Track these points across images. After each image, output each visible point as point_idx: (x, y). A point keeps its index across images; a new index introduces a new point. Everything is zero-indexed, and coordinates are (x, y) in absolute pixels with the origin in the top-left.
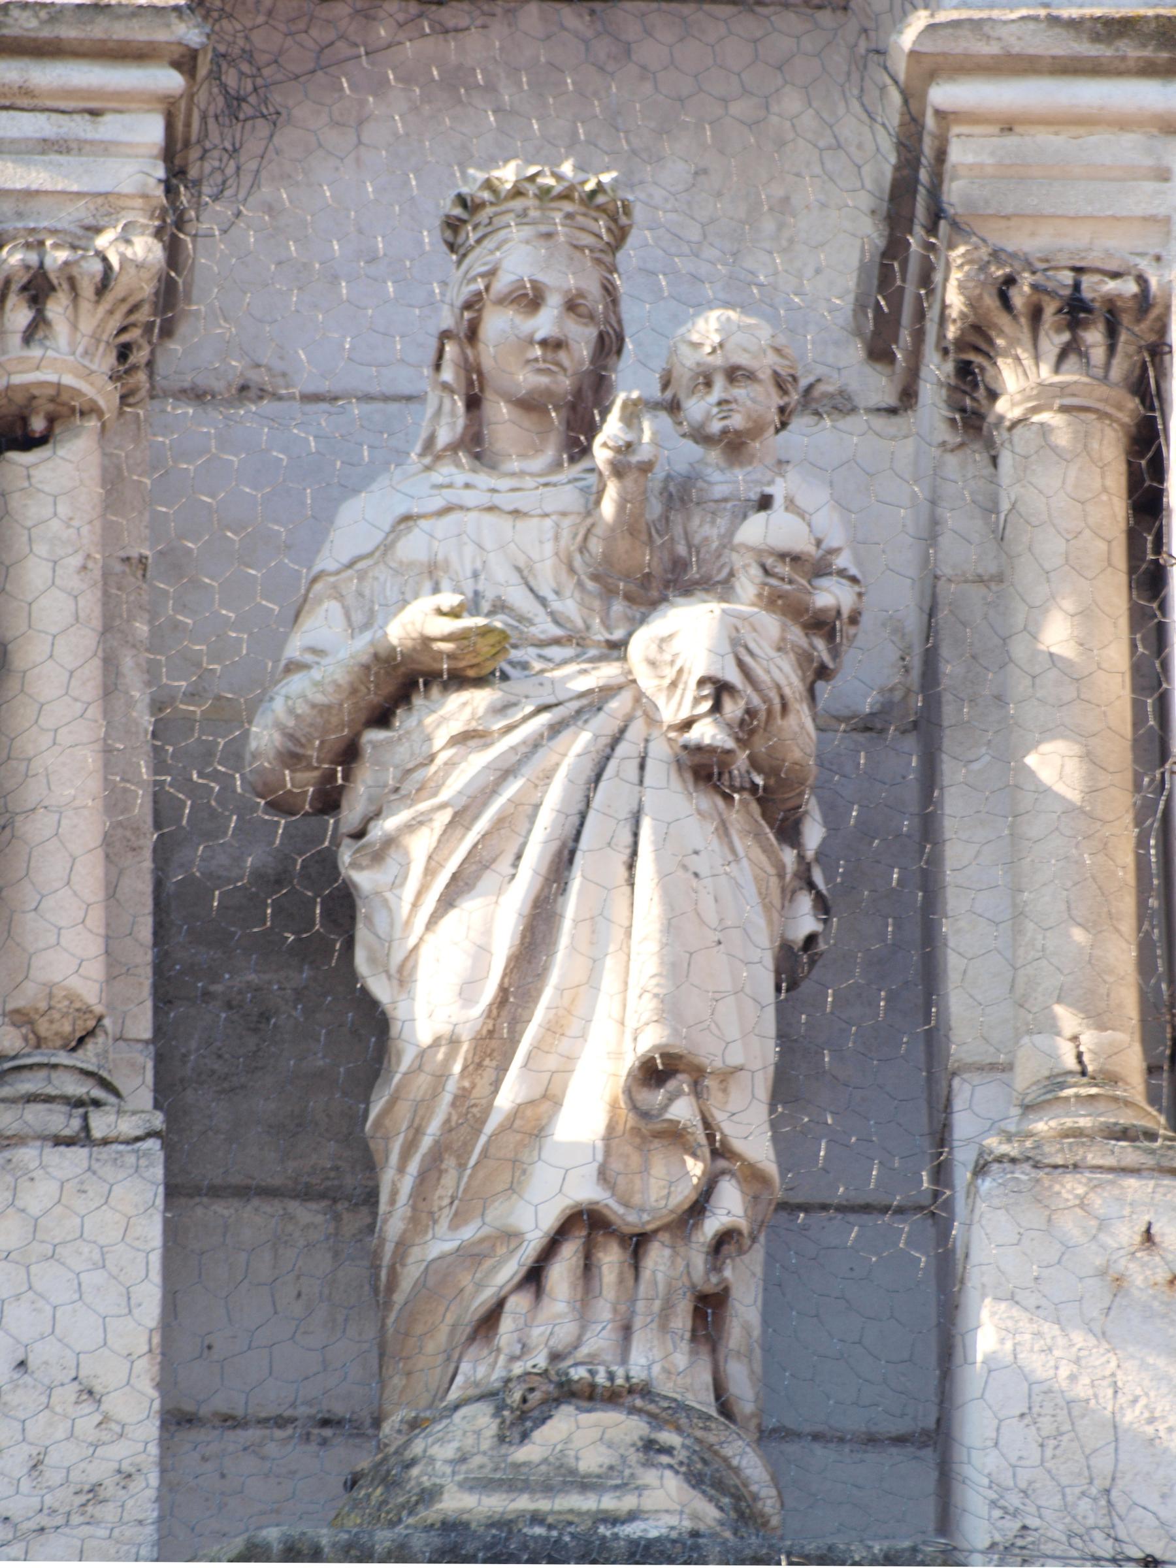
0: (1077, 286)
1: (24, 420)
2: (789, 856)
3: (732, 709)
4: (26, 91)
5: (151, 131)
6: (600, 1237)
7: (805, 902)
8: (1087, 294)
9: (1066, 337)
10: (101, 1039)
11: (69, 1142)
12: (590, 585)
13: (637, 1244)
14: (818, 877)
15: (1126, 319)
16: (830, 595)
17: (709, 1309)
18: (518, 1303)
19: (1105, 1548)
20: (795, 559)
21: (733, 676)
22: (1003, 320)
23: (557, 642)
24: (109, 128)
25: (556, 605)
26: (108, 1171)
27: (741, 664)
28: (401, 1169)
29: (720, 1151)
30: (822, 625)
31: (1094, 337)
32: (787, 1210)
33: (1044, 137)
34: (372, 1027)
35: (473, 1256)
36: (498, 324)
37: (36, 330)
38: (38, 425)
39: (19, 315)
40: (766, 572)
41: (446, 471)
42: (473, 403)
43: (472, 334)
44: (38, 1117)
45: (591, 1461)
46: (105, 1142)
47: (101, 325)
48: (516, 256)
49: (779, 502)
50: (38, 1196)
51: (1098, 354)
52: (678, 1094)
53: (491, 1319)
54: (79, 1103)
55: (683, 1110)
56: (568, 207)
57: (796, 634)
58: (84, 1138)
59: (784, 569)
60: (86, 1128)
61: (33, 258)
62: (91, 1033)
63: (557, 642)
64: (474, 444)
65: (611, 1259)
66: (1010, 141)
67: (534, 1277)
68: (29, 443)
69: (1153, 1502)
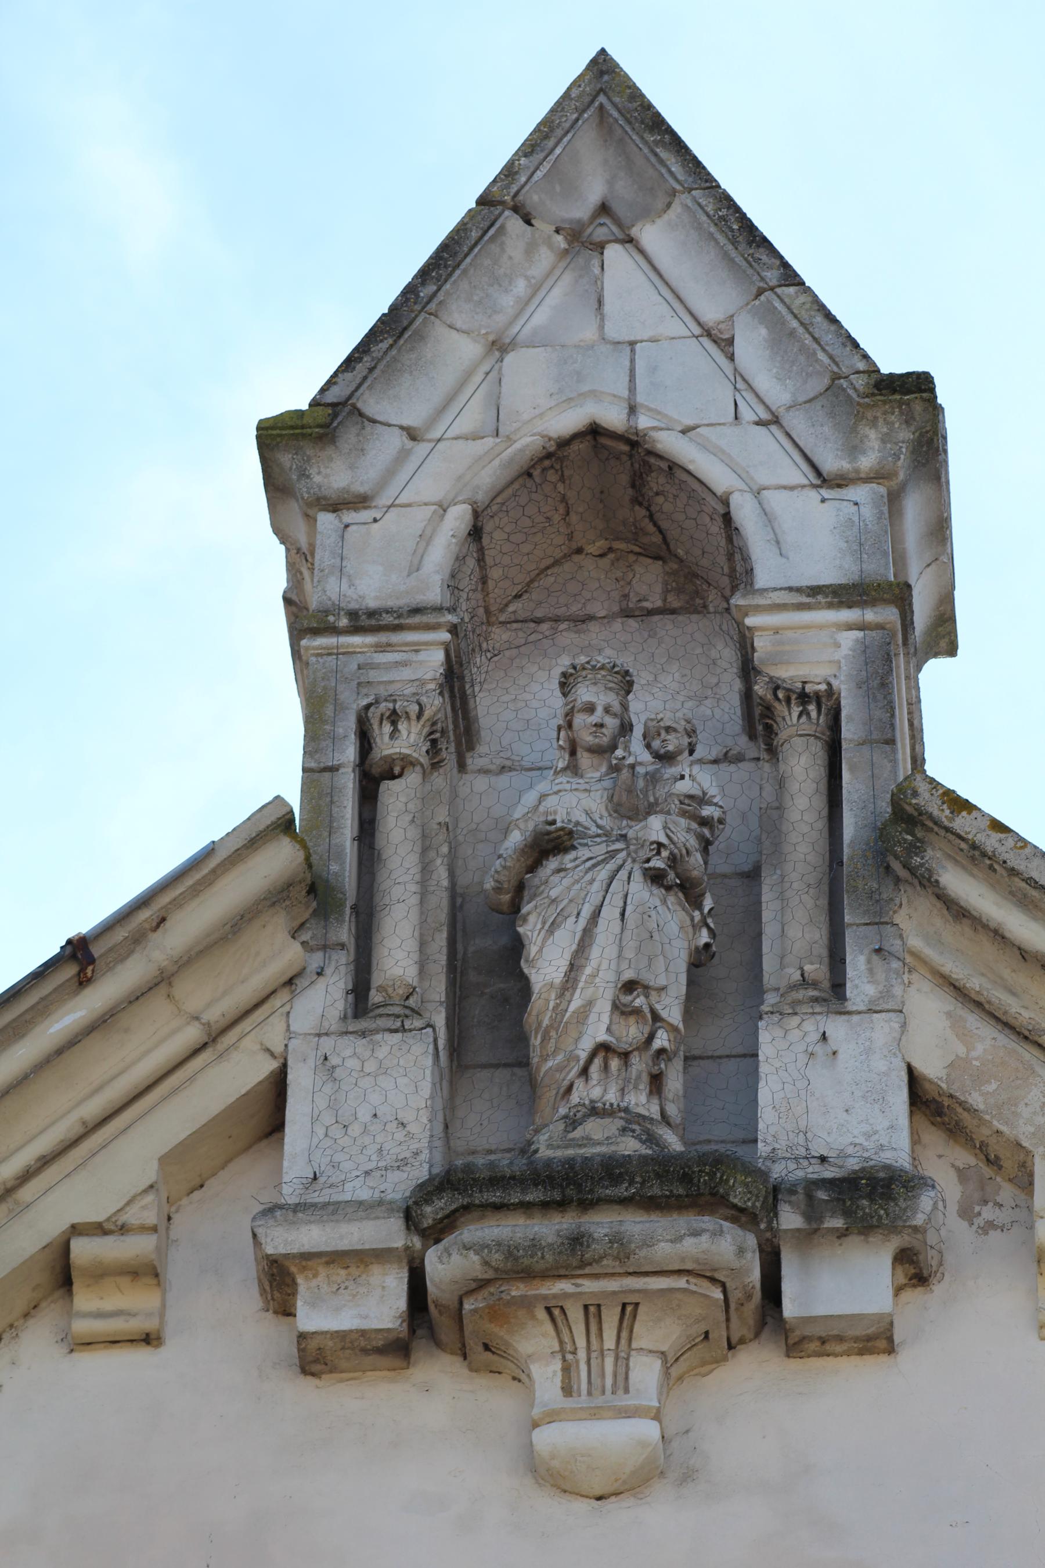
0: (804, 688)
1: (392, 769)
2: (697, 914)
3: (665, 853)
4: (389, 645)
5: (439, 656)
6: (610, 1055)
7: (705, 932)
8: (807, 690)
9: (801, 708)
10: (415, 996)
11: (396, 1031)
12: (615, 815)
13: (625, 1056)
14: (709, 921)
15: (824, 700)
16: (707, 811)
17: (656, 1082)
18: (579, 1084)
19: (802, 1152)
20: (691, 797)
21: (663, 840)
22: (776, 704)
23: (598, 836)
24: (422, 656)
25: (599, 822)
26: (411, 1041)
27: (668, 836)
28: (536, 1038)
29: (656, 1017)
30: (704, 822)
31: (812, 708)
33: (790, 634)
35: (560, 1068)
36: (579, 719)
37: (394, 734)
38: (397, 770)
39: (387, 728)
40: (681, 803)
41: (562, 779)
42: (573, 753)
43: (570, 725)
44: (382, 1023)
45: (597, 1136)
46: (410, 1030)
47: (421, 731)
48: (584, 693)
49: (687, 777)
50: (382, 1052)
51: (814, 714)
52: (638, 996)
53: (569, 1089)
54: (398, 1016)
55: (640, 1001)
56: (603, 673)
57: (694, 825)
58: (403, 1029)
59: (687, 801)
60: (403, 1026)
61: (391, 705)
62: (411, 994)
63: (598, 836)
64: (573, 768)
65: (615, 1063)
66: (778, 637)
67: (585, 1072)
68: (393, 777)
69: (825, 1136)
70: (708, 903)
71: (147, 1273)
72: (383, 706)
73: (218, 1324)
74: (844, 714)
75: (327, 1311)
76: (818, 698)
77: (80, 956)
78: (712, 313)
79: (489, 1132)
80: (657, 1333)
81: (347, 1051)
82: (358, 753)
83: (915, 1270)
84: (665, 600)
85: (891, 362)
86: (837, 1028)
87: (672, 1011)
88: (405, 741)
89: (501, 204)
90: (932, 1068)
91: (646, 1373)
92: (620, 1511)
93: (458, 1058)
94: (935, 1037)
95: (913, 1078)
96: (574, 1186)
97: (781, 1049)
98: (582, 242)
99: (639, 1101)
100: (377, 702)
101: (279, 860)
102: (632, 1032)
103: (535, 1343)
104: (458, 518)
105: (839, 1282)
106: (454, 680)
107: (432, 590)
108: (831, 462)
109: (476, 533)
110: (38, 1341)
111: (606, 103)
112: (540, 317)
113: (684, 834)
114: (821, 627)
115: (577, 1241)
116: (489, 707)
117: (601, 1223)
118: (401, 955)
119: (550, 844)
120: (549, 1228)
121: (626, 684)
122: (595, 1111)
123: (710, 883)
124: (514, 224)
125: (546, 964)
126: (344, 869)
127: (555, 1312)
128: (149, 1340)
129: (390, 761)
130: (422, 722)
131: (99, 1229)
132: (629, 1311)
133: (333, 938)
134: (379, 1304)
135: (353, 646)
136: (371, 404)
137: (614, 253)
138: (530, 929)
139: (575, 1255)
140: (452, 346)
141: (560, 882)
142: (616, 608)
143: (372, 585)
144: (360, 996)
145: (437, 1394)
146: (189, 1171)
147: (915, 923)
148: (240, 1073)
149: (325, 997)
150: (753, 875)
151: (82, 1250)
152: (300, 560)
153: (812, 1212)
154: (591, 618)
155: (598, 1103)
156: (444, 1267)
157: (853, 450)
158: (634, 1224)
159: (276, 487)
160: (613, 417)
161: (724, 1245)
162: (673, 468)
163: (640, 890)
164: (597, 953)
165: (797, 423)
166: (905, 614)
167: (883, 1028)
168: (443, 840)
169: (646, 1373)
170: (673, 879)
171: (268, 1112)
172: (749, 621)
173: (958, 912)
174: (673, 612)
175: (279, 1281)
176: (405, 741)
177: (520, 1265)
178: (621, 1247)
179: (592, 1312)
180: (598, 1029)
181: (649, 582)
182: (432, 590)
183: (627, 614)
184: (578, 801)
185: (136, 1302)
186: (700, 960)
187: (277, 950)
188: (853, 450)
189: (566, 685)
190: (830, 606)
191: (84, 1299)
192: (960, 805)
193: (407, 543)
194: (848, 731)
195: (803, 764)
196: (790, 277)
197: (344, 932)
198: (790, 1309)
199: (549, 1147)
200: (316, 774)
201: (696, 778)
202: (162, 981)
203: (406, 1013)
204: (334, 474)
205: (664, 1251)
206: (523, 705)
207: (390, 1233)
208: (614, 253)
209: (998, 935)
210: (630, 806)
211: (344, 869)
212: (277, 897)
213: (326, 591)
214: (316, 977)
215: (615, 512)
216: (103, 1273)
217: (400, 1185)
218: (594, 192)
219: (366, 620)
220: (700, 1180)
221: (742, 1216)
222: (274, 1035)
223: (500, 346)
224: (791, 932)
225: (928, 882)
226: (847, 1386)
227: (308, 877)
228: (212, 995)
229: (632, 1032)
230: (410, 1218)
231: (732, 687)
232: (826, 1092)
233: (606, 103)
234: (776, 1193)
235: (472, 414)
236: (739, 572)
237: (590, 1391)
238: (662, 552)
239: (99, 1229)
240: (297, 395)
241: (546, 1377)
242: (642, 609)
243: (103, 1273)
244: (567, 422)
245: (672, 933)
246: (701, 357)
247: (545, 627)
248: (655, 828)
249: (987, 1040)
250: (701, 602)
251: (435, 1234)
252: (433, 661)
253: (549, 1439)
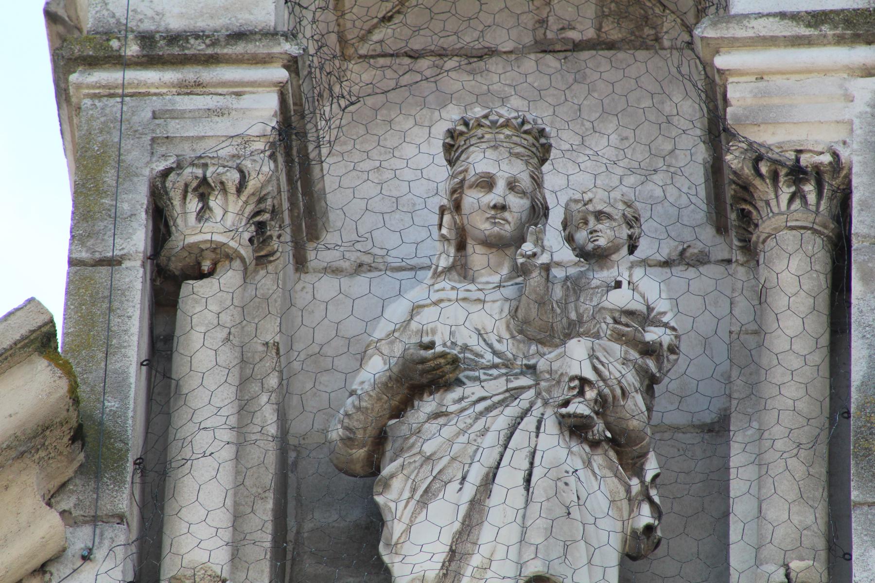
0: (798, 160)
1: (199, 264)
2: (635, 482)
3: (590, 394)
4: (199, 84)
5: (270, 102)
7: (646, 509)
9: (793, 189)
12: (519, 337)
14: (653, 492)
15: (827, 177)
16: (652, 335)
20: (630, 313)
21: (590, 374)
22: (757, 182)
23: (495, 366)
24: (246, 102)
25: (497, 346)
27: (595, 369)
30: (649, 350)
31: (809, 188)
36: (472, 199)
37: (203, 213)
38: (206, 266)
39: (194, 204)
40: (616, 321)
42: (461, 247)
43: (457, 206)
48: (479, 160)
49: (625, 284)
51: (812, 198)
56: (507, 132)
57: (634, 355)
59: (624, 320)
61: (199, 172)
63: (495, 366)
64: (461, 269)
66: (761, 84)
68: (201, 276)
70: (652, 467)
72: (189, 173)
74: (856, 198)
76: (818, 174)
84: (599, 29)
88: (221, 224)
100: (179, 166)
106: (291, 137)
113: (619, 367)
114: (826, 72)
116: (342, 179)
119: (425, 376)
121: (540, 149)
126: (126, 405)
129: (197, 251)
130: (243, 198)
133: (106, 507)
135: (145, 84)
138: (394, 498)
141: (438, 431)
142: (528, 39)
150: (718, 429)
154: (492, 52)
163: (553, 446)
168: (272, 366)
172: (720, 62)
174: (611, 46)
176: (221, 224)
183: (544, 48)
184: (469, 317)
189: (453, 147)
190: (840, 40)
195: (793, 270)
197: (124, 498)
200: (89, 268)
201: (638, 286)
206: (392, 175)
210: (543, 324)
211: (126, 405)
214: (80, 562)
219: (163, 49)
231: (693, 156)
242: (565, 40)
247: (424, 64)
250: (652, 32)
252: (261, 110)
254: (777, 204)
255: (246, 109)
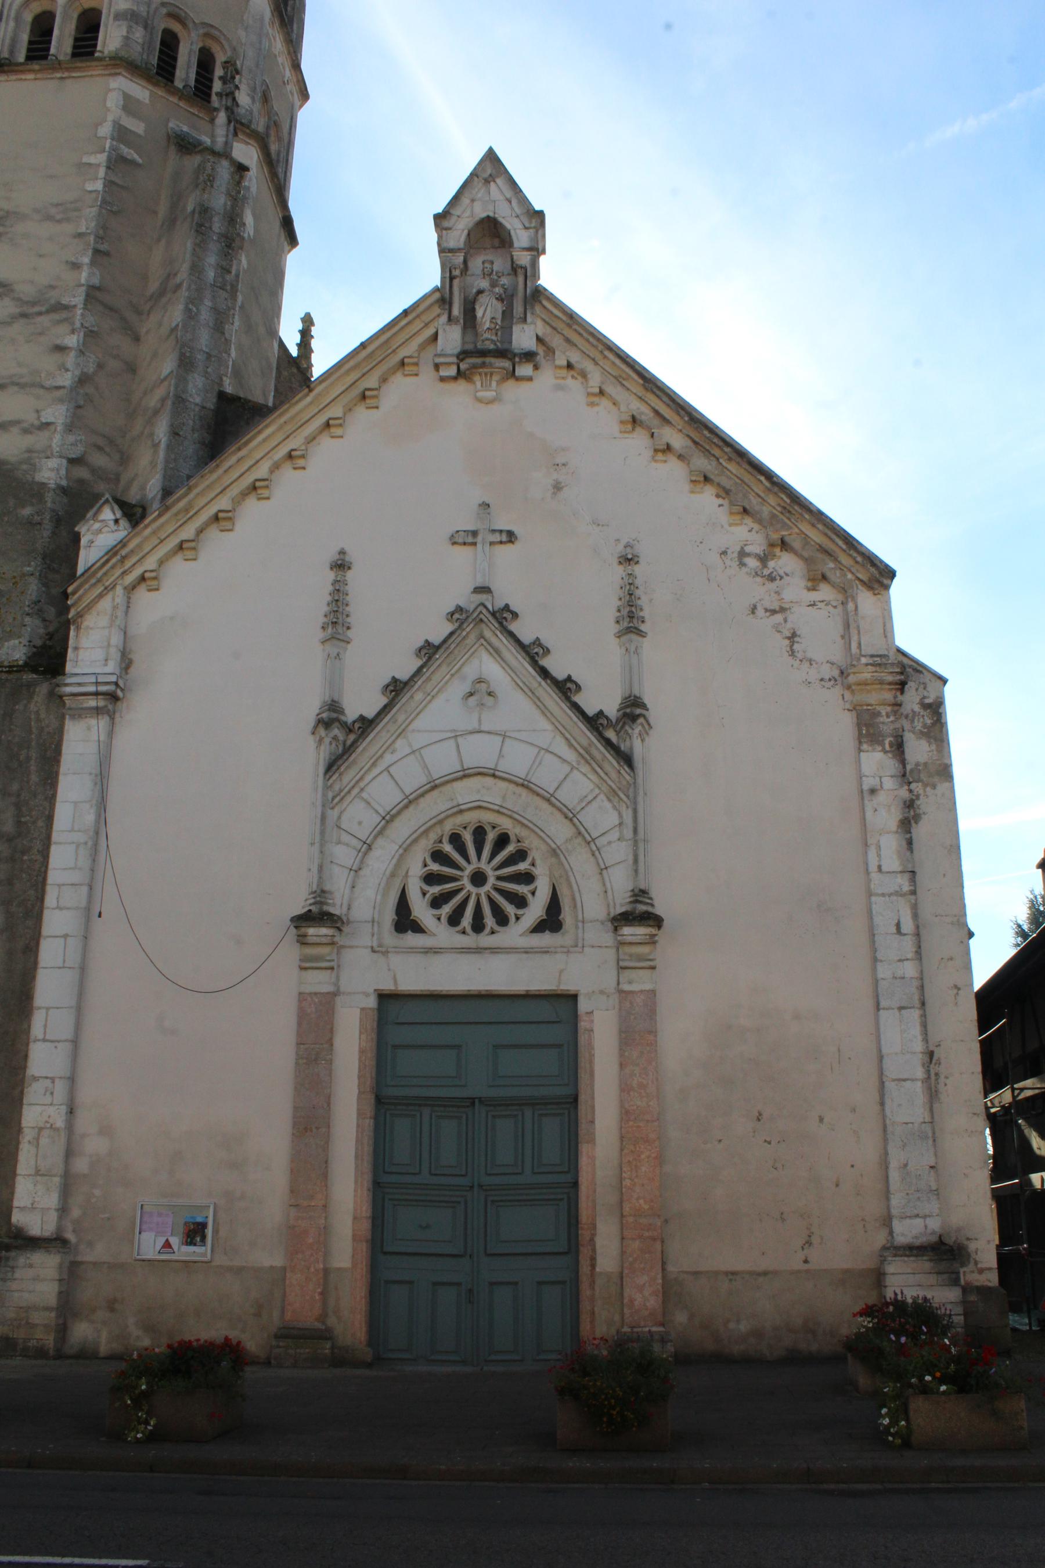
32: (502, 328)
34: (475, 317)
48: (486, 265)
71: (416, 364)
73: (427, 374)
75: (445, 372)
77: (406, 313)
78: (508, 196)
79: (470, 347)
80: (495, 378)
81: (447, 328)
82: (447, 269)
83: (536, 367)
85: (537, 208)
86: (525, 327)
87: (499, 322)
88: (457, 273)
89: (474, 175)
90: (540, 334)
91: (494, 384)
92: (490, 406)
93: (465, 328)
94: (540, 329)
95: (537, 336)
96: (483, 353)
97: (516, 329)
98: (487, 181)
99: (494, 338)
101: (437, 295)
102: (493, 326)
103: (477, 378)
104: (466, 232)
105: (525, 369)
106: (465, 262)
107: (462, 246)
108: (527, 225)
109: (469, 234)
110: (399, 374)
111: (491, 157)
112: (480, 195)
113: (502, 291)
115: (484, 363)
116: (470, 264)
117: (488, 360)
118: (456, 311)
119: (480, 292)
120: (479, 360)
121: (492, 263)
122: (487, 339)
123: (506, 299)
124: (476, 178)
125: (479, 313)
126: (447, 296)
127: (480, 374)
128: (416, 375)
131: (409, 357)
132: (491, 374)
134: (452, 371)
136: (452, 211)
137: (492, 183)
138: (477, 307)
139: (483, 365)
140: (465, 200)
141: (483, 299)
143: (452, 244)
144: (450, 319)
145: (462, 385)
146: (422, 347)
147: (538, 309)
148: (429, 332)
149: (444, 318)
150: (512, 296)
151: (406, 360)
152: (440, 237)
153: (521, 359)
155: (488, 339)
156: (463, 366)
157: (531, 223)
158: (493, 360)
159: (437, 225)
160: (491, 214)
161: (507, 364)
162: (501, 224)
163: (495, 301)
164: (488, 311)
165: (522, 217)
166: (537, 250)
167: (533, 326)
168: (463, 289)
169: (494, 384)
170: (500, 299)
171: (435, 337)
173: (544, 307)
175: (437, 367)
176: (457, 273)
177: (474, 367)
178: (491, 365)
179: (486, 374)
180: (487, 325)
181: (496, 242)
182: (462, 246)
184: (484, 284)
185: (414, 369)
186: (504, 312)
187: (437, 310)
188: (531, 223)
189: (483, 263)
191: (406, 368)
192: (546, 290)
193: (458, 238)
194: (529, 274)
195: (521, 279)
196: (521, 191)
197: (447, 307)
198: (517, 374)
199: (479, 346)
200: (443, 279)
201: (504, 281)
202: (418, 316)
203: (457, 322)
204: (446, 224)
205: (497, 365)
206: (477, 264)
207: (455, 360)
208: (492, 183)
209: (552, 313)
210: (494, 284)
211: (447, 296)
212: (437, 301)
213: (444, 245)
215: (491, 233)
216: (409, 364)
217: (456, 351)
218: (489, 172)
219: (451, 251)
220: (503, 353)
221: (510, 359)
222: (436, 324)
223: (473, 201)
224: (518, 309)
225: (540, 302)
226: (525, 386)
227: (441, 298)
228: (426, 318)
229: (493, 326)
230: (458, 357)
231: (510, 263)
232: (523, 338)
233: (491, 157)
234: (515, 355)
235: (468, 213)
236: (511, 244)
237: (486, 387)
238: (499, 237)
239: (409, 357)
240: (440, 209)
241: (478, 384)
243: (409, 364)
244: (484, 215)
245: (499, 307)
246: (506, 204)
248: (497, 290)
249: (549, 330)
251: (462, 360)
252: (462, 258)
253: (480, 394)
254: (519, 270)
255: (460, 258)
